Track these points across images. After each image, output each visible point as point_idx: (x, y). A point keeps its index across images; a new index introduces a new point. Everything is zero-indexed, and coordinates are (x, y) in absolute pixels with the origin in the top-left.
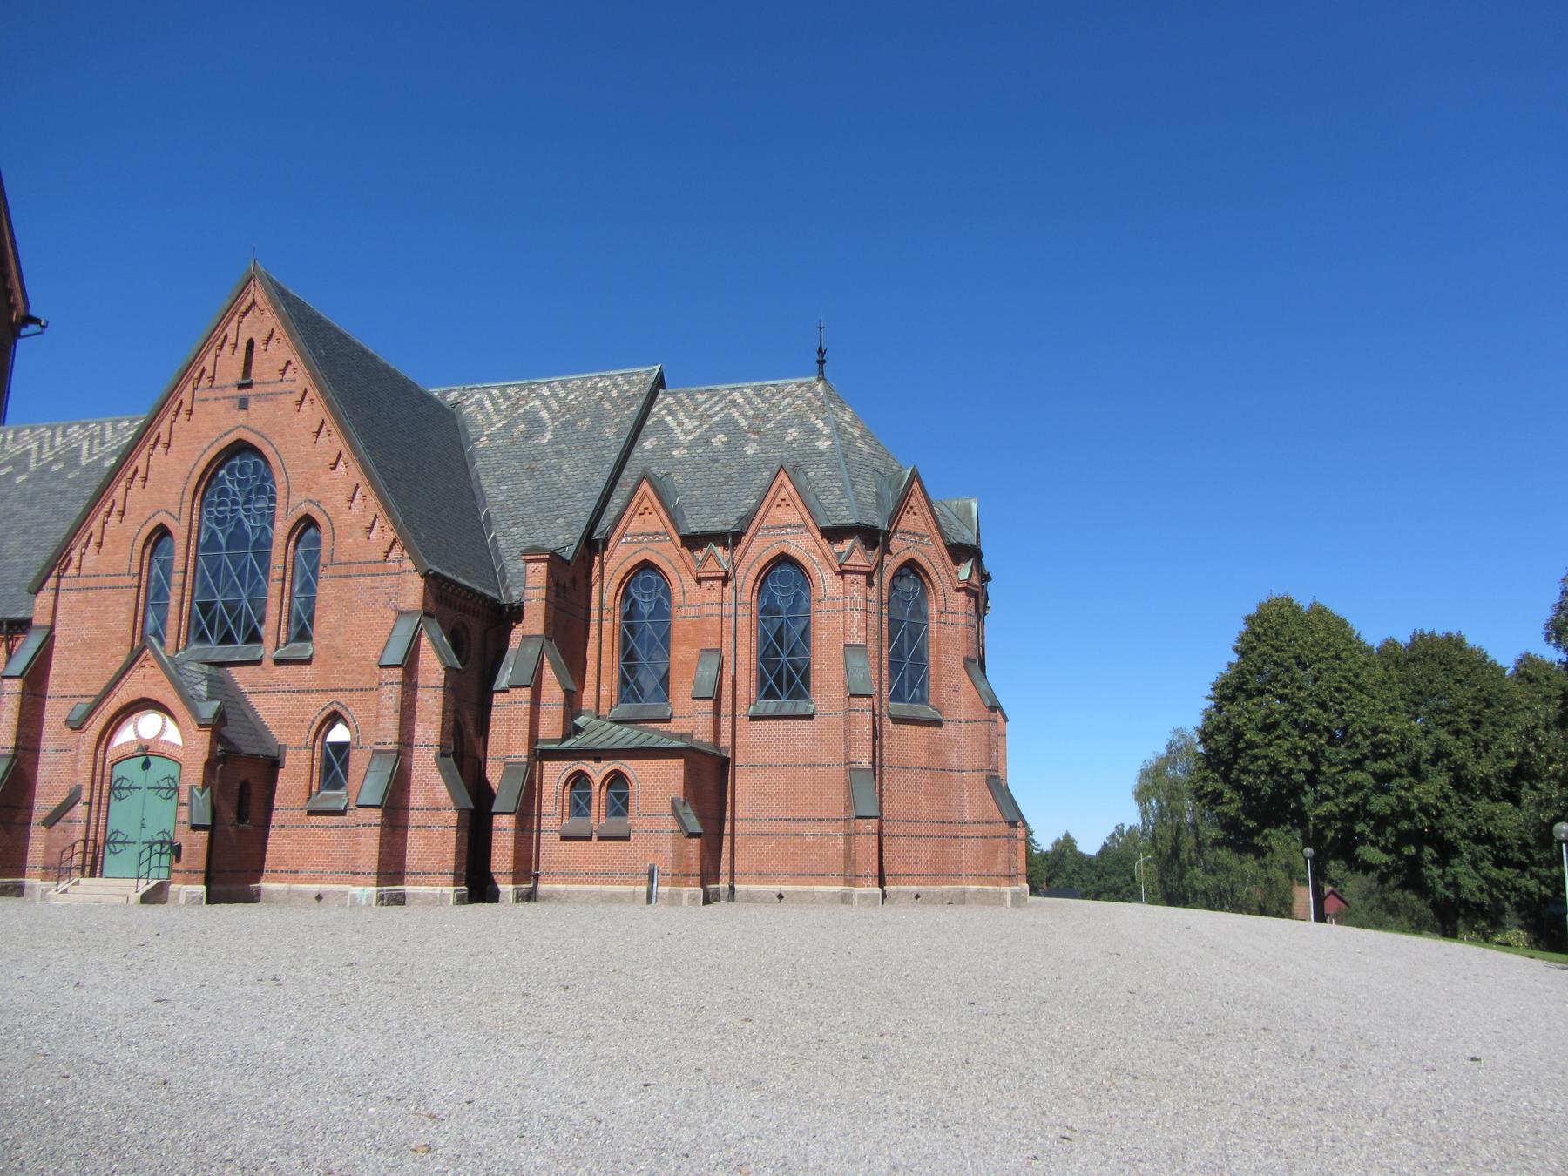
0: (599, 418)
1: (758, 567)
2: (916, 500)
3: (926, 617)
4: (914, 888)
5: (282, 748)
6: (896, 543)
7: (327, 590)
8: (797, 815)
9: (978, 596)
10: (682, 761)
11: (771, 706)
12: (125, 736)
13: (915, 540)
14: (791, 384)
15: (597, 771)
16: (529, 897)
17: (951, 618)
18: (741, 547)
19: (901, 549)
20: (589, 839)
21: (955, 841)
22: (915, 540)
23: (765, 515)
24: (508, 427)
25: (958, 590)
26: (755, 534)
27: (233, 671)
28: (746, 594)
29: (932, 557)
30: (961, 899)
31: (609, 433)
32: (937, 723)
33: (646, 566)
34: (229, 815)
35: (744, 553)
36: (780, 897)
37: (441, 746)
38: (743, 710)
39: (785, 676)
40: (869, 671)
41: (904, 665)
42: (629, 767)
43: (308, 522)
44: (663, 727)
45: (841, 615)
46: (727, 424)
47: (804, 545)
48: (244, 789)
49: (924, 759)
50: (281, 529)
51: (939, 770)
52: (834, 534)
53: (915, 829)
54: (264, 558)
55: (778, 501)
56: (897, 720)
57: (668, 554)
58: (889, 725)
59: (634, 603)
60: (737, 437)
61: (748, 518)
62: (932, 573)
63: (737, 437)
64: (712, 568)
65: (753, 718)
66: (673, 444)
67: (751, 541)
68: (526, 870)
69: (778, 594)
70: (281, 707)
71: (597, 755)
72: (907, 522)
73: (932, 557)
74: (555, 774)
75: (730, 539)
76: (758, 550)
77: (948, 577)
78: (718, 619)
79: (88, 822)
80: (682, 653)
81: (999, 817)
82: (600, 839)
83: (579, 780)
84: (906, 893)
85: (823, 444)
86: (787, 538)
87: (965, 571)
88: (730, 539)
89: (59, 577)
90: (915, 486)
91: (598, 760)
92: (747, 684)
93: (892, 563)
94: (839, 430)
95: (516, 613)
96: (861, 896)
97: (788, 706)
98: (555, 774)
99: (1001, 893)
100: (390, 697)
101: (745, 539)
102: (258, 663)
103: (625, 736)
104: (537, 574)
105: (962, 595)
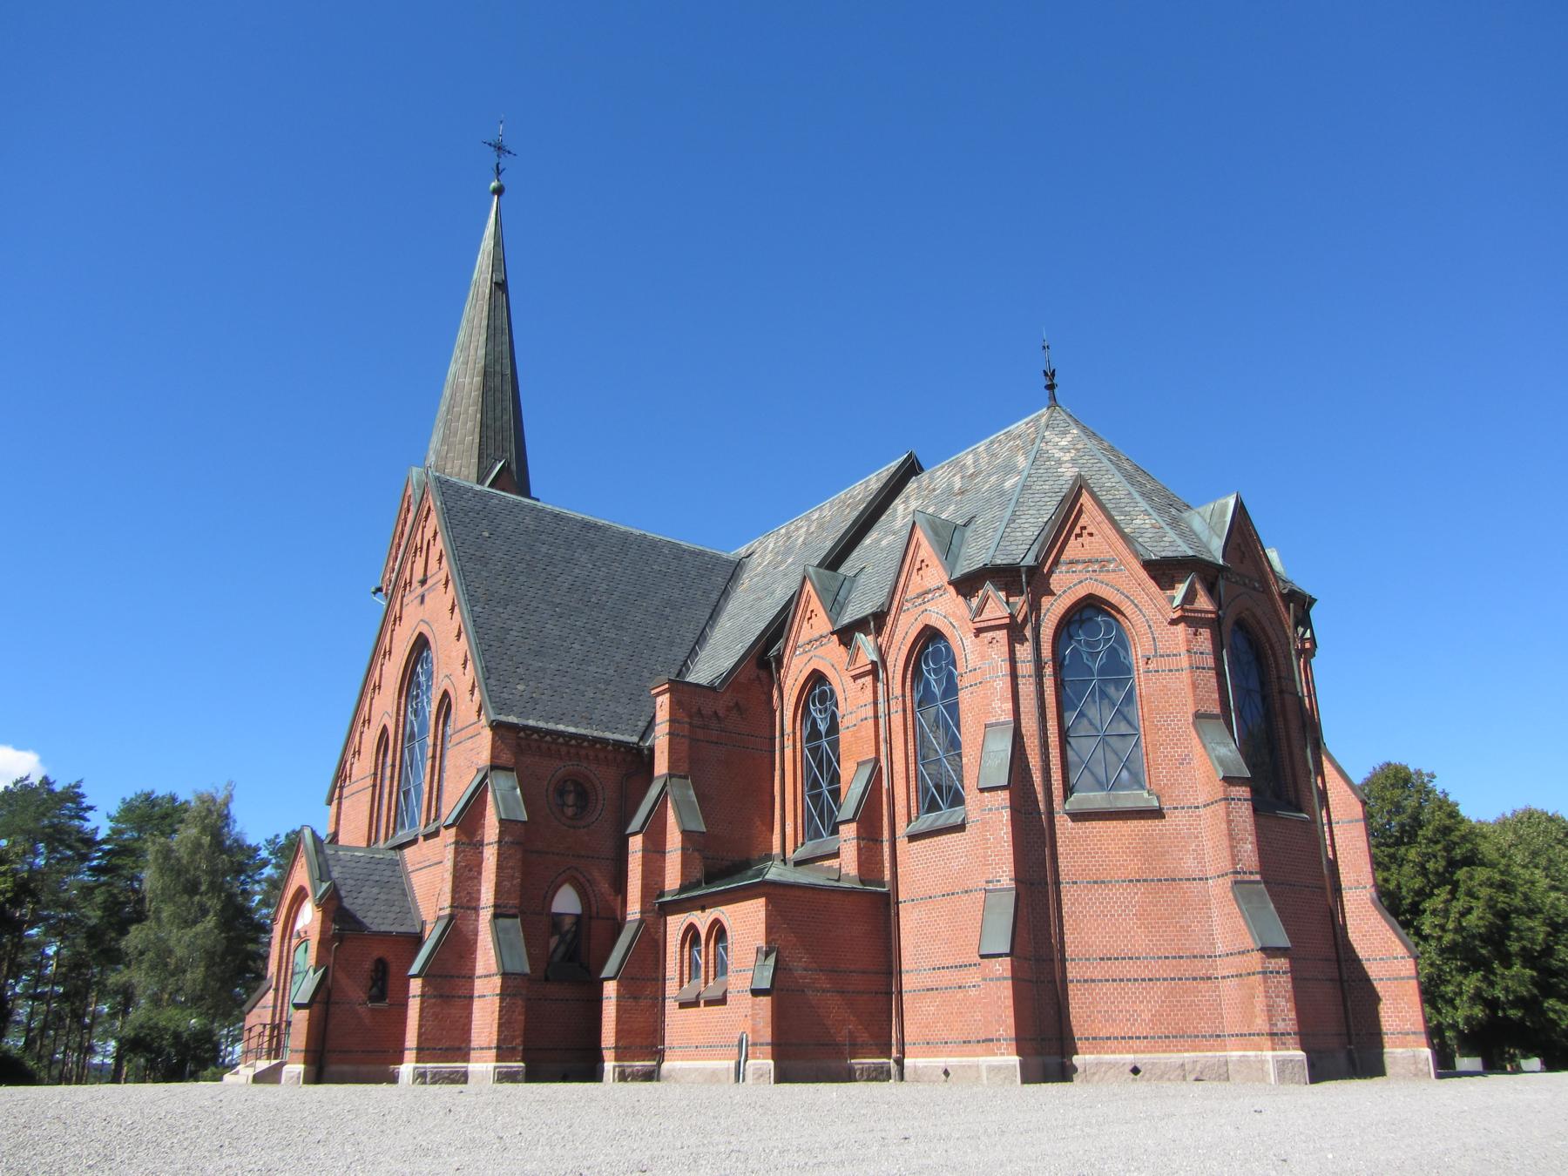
1: (905, 650)
2: (1091, 515)
3: (1128, 670)
4: (1129, 1058)
5: (423, 923)
6: (1057, 581)
8: (959, 961)
10: (762, 901)
11: (928, 821)
13: (1098, 566)
14: (1020, 426)
15: (702, 920)
16: (650, 1076)
17: (1164, 663)
18: (887, 630)
19: (1067, 587)
20: (695, 1004)
21: (1202, 986)
23: (906, 586)
25: (1174, 622)
26: (900, 609)
27: (407, 851)
30: (1223, 1074)
32: (1157, 814)
34: (355, 991)
35: (891, 635)
36: (946, 1073)
37: (496, 906)
38: (902, 830)
44: (834, 863)
47: (948, 612)
48: (381, 967)
49: (1133, 867)
51: (1163, 881)
53: (1130, 969)
55: (918, 565)
56: (1078, 816)
57: (831, 658)
58: (1064, 825)
59: (814, 722)
62: (1127, 608)
65: (912, 838)
67: (896, 620)
68: (646, 1047)
69: (932, 678)
75: (877, 621)
76: (904, 630)
78: (871, 722)
79: (275, 1007)
80: (847, 770)
81: (1249, 942)
82: (709, 1003)
83: (691, 934)
84: (1112, 1065)
86: (927, 606)
89: (342, 788)
90: (1085, 498)
91: (703, 909)
92: (902, 794)
93: (1053, 610)
96: (991, 1068)
97: (947, 816)
99: (1263, 1062)
101: (890, 620)
102: (414, 841)
105: (1181, 627)
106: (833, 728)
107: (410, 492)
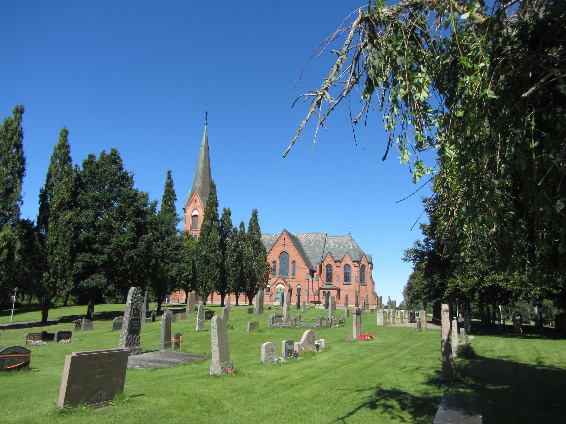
0: (319, 241)
2: (364, 256)
7: (297, 270)
9: (371, 268)
12: (277, 287)
13: (364, 262)
15: (327, 291)
19: (362, 263)
22: (364, 262)
24: (306, 241)
28: (343, 269)
29: (366, 264)
31: (322, 244)
33: (329, 264)
38: (343, 283)
39: (347, 279)
40: (358, 279)
41: (362, 279)
42: (330, 291)
43: (294, 261)
45: (355, 272)
46: (337, 243)
47: (350, 263)
50: (290, 262)
52: (354, 262)
54: (288, 265)
57: (332, 263)
60: (339, 245)
61: (342, 259)
63: (339, 245)
64: (338, 265)
66: (330, 246)
70: (293, 284)
71: (327, 289)
72: (363, 259)
73: (366, 264)
74: (321, 291)
75: (340, 262)
76: (344, 263)
77: (368, 266)
83: (324, 292)
85: (351, 247)
87: (370, 265)
88: (340, 262)
92: (343, 280)
93: (361, 265)
94: (353, 245)
95: (316, 271)
97: (348, 283)
98: (321, 291)
100: (307, 283)
103: (328, 287)
104: (318, 267)
106: (331, 270)
107: (196, 192)
